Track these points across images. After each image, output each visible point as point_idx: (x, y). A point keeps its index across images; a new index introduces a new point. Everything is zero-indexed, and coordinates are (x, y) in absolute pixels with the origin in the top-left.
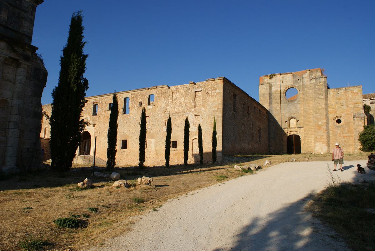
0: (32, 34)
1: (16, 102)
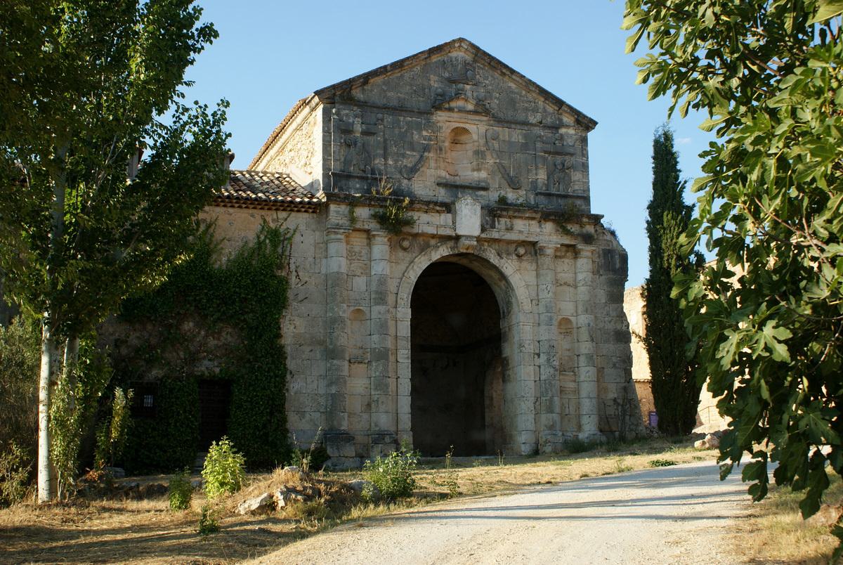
0: (588, 190)
1: (584, 319)
